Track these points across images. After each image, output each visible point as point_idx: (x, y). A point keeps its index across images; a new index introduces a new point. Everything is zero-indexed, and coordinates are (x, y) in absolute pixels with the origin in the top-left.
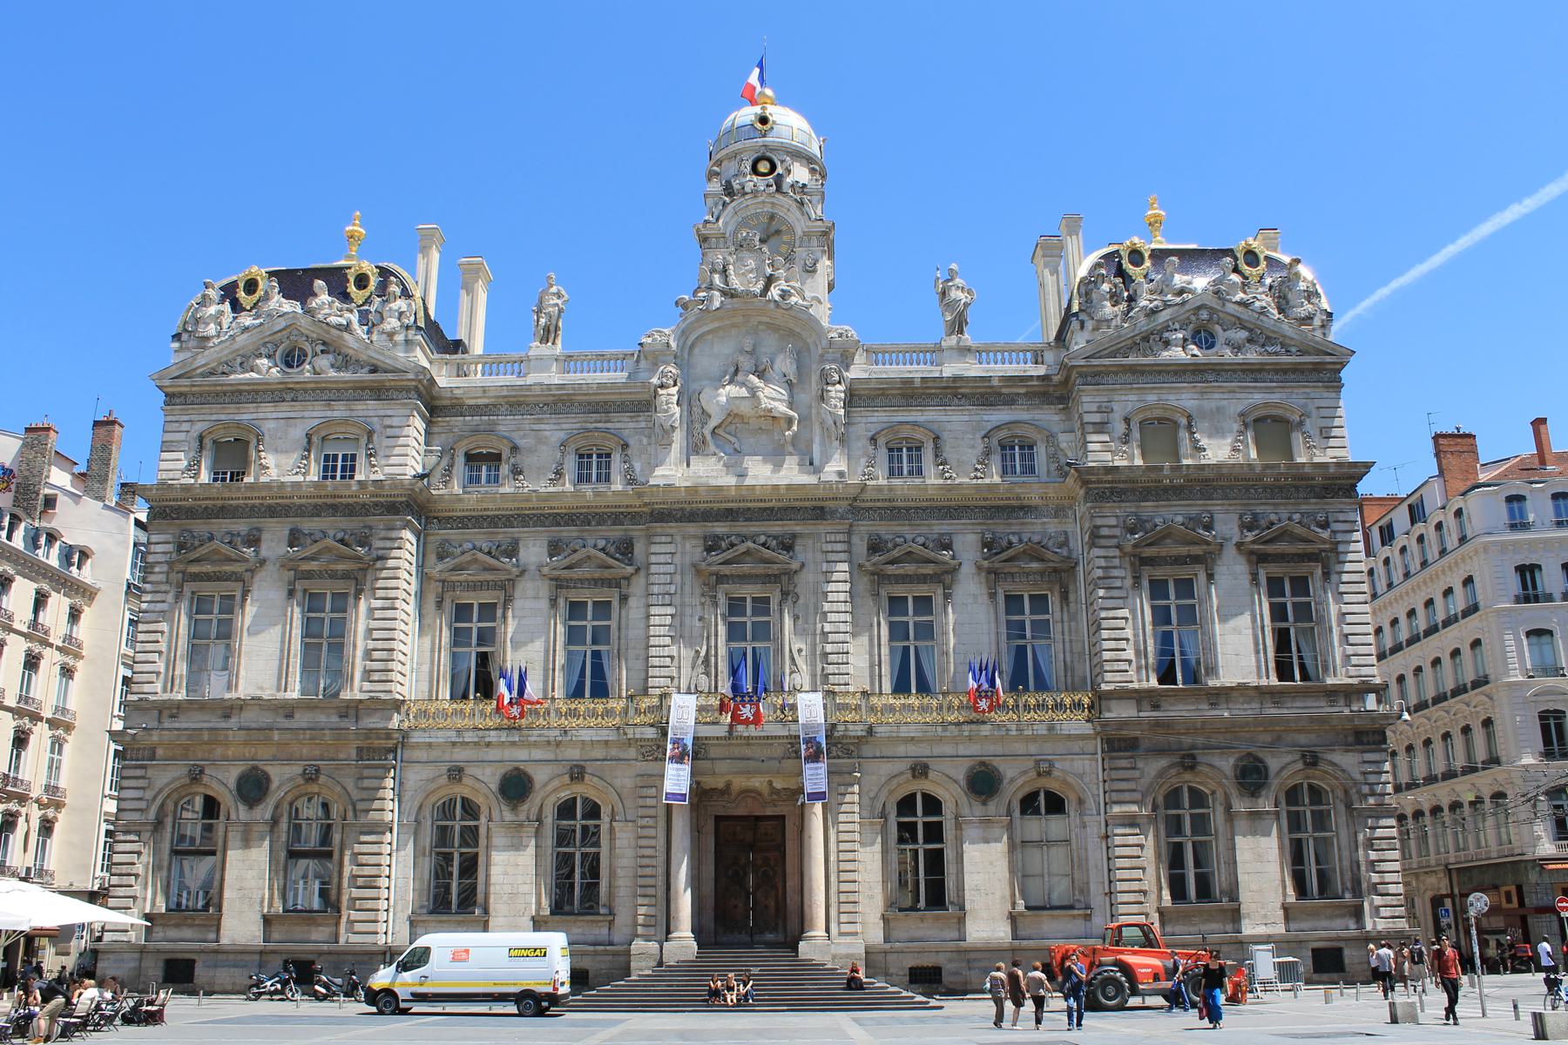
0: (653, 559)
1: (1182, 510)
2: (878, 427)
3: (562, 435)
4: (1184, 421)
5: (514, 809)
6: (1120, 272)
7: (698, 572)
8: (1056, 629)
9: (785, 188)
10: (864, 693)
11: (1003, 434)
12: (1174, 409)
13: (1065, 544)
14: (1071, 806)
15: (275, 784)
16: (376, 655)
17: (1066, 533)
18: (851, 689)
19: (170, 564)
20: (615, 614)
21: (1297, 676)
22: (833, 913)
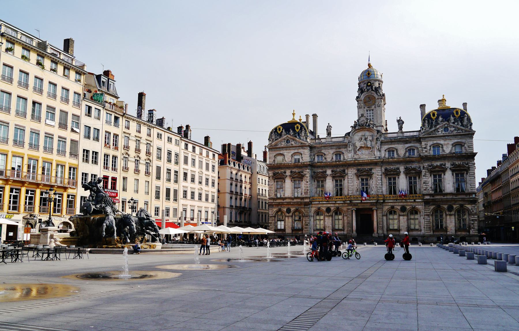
0: (349, 173)
1: (440, 163)
2: (387, 148)
3: (333, 152)
4: (441, 146)
5: (328, 213)
6: (431, 118)
7: (356, 175)
8: (418, 183)
9: (374, 89)
10: (384, 195)
11: (409, 148)
12: (439, 144)
13: (420, 168)
14: (419, 213)
15: (292, 210)
16: (306, 190)
17: (420, 166)
18: (382, 194)
19: (273, 176)
20: (343, 182)
21: (460, 191)
22: (378, 230)
